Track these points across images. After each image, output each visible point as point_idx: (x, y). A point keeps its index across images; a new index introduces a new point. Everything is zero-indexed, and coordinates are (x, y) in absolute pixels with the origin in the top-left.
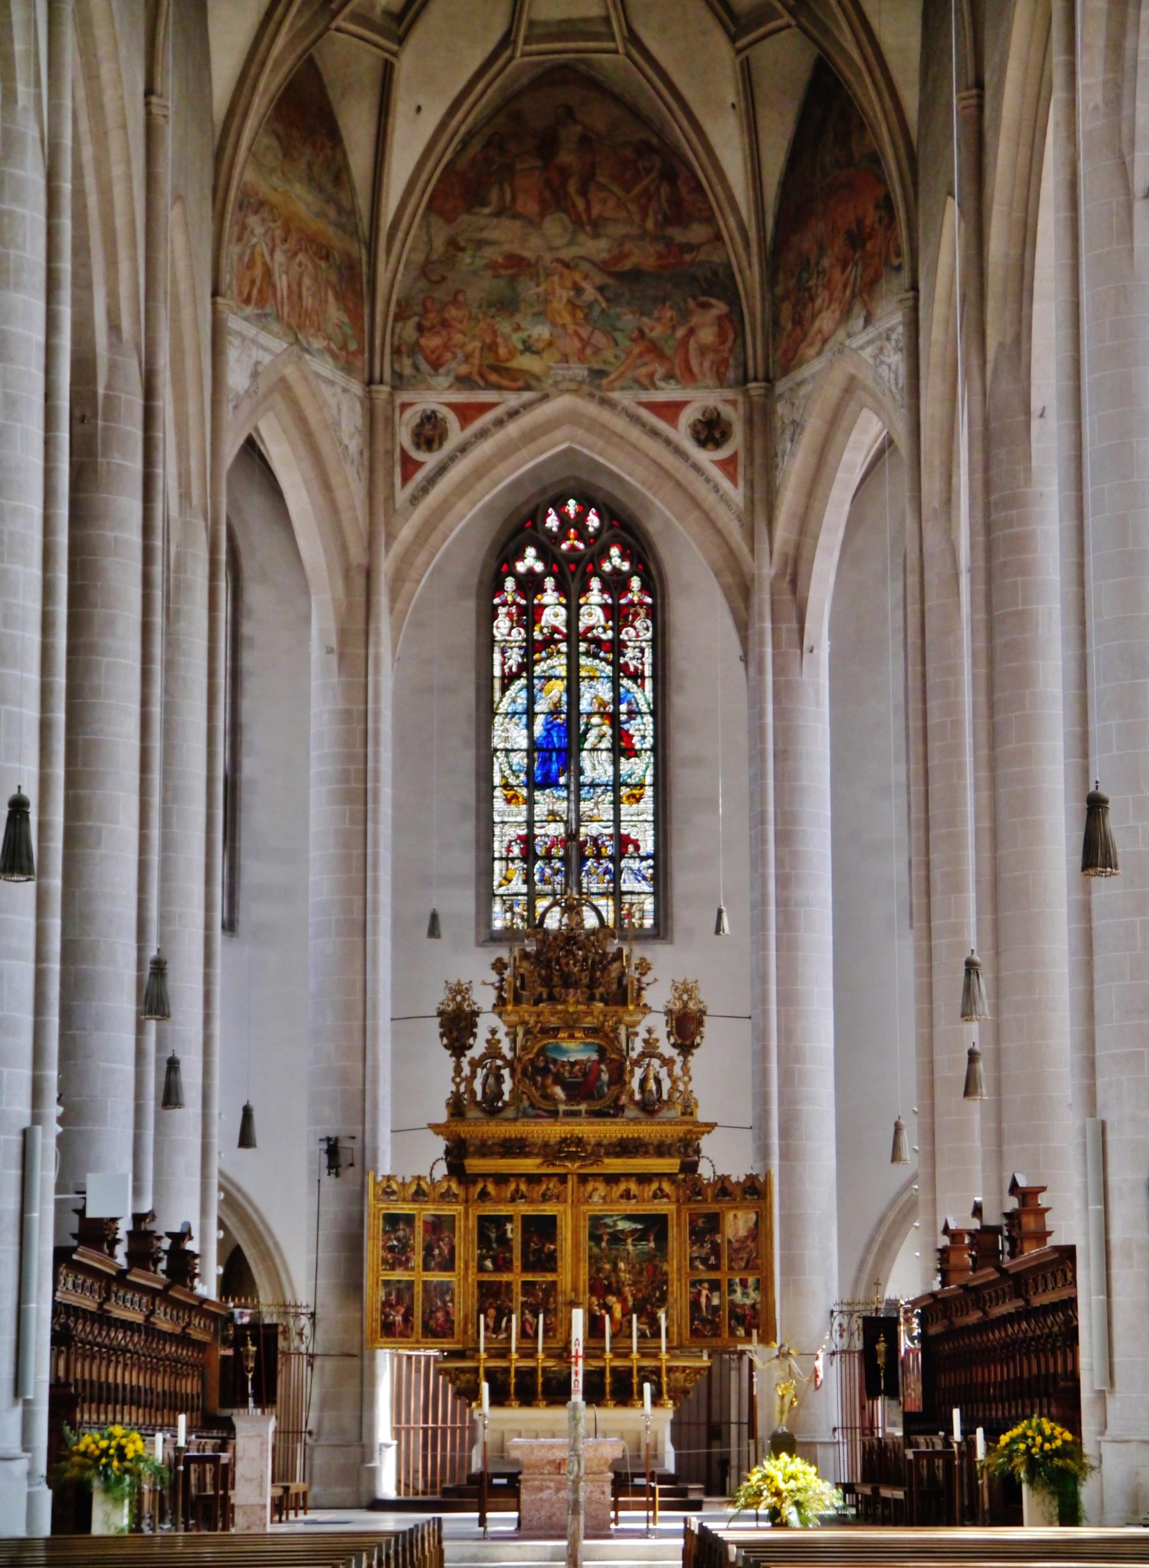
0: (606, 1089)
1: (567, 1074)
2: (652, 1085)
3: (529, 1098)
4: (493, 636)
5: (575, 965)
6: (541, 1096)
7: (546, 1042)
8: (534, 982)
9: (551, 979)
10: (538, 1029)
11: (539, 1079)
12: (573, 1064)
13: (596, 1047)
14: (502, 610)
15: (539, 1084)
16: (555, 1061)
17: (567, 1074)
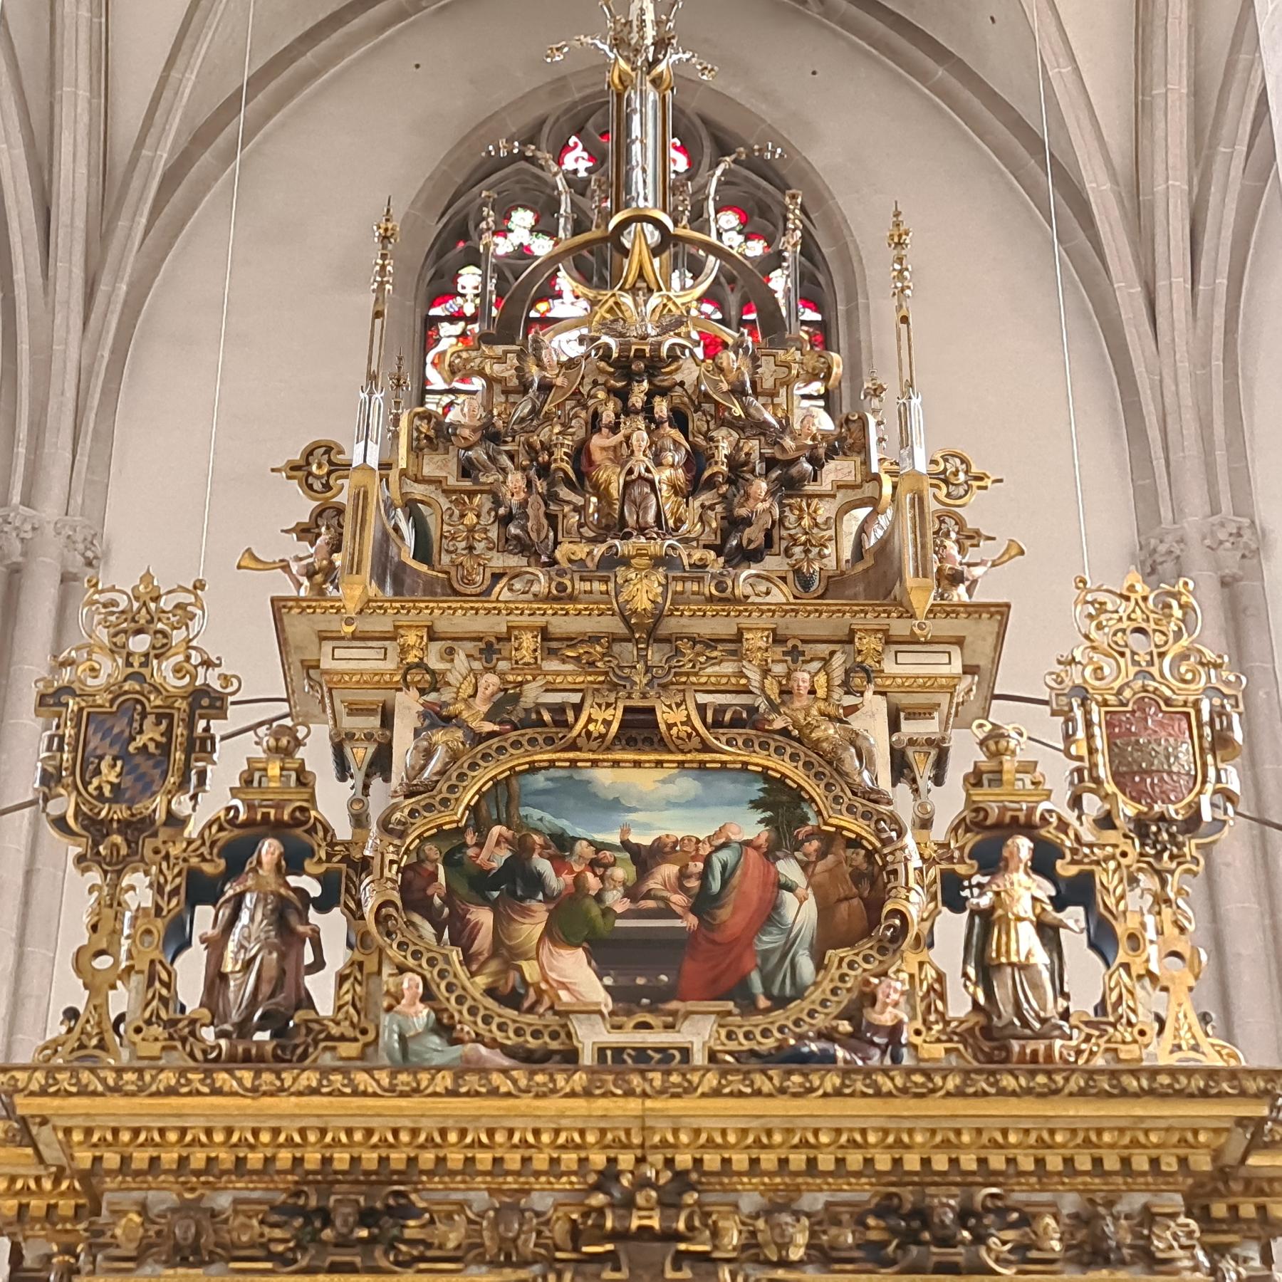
0: (806, 966)
1: (616, 900)
2: (1026, 942)
3: (428, 996)
4: (425, 381)
5: (659, 463)
6: (490, 992)
7: (519, 760)
8: (471, 530)
9: (552, 519)
10: (482, 707)
11: (484, 917)
12: (645, 859)
13: (756, 790)
14: (446, 329)
15: (483, 941)
16: (561, 844)
17: (616, 900)
